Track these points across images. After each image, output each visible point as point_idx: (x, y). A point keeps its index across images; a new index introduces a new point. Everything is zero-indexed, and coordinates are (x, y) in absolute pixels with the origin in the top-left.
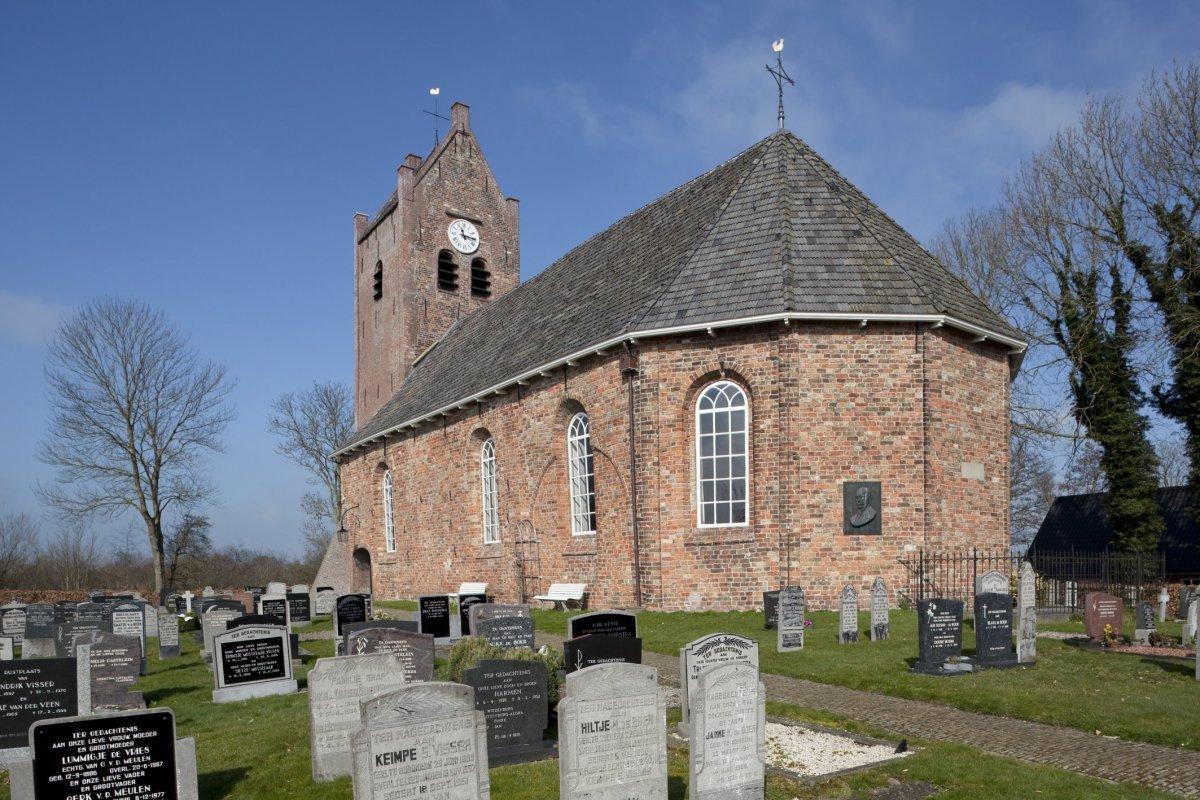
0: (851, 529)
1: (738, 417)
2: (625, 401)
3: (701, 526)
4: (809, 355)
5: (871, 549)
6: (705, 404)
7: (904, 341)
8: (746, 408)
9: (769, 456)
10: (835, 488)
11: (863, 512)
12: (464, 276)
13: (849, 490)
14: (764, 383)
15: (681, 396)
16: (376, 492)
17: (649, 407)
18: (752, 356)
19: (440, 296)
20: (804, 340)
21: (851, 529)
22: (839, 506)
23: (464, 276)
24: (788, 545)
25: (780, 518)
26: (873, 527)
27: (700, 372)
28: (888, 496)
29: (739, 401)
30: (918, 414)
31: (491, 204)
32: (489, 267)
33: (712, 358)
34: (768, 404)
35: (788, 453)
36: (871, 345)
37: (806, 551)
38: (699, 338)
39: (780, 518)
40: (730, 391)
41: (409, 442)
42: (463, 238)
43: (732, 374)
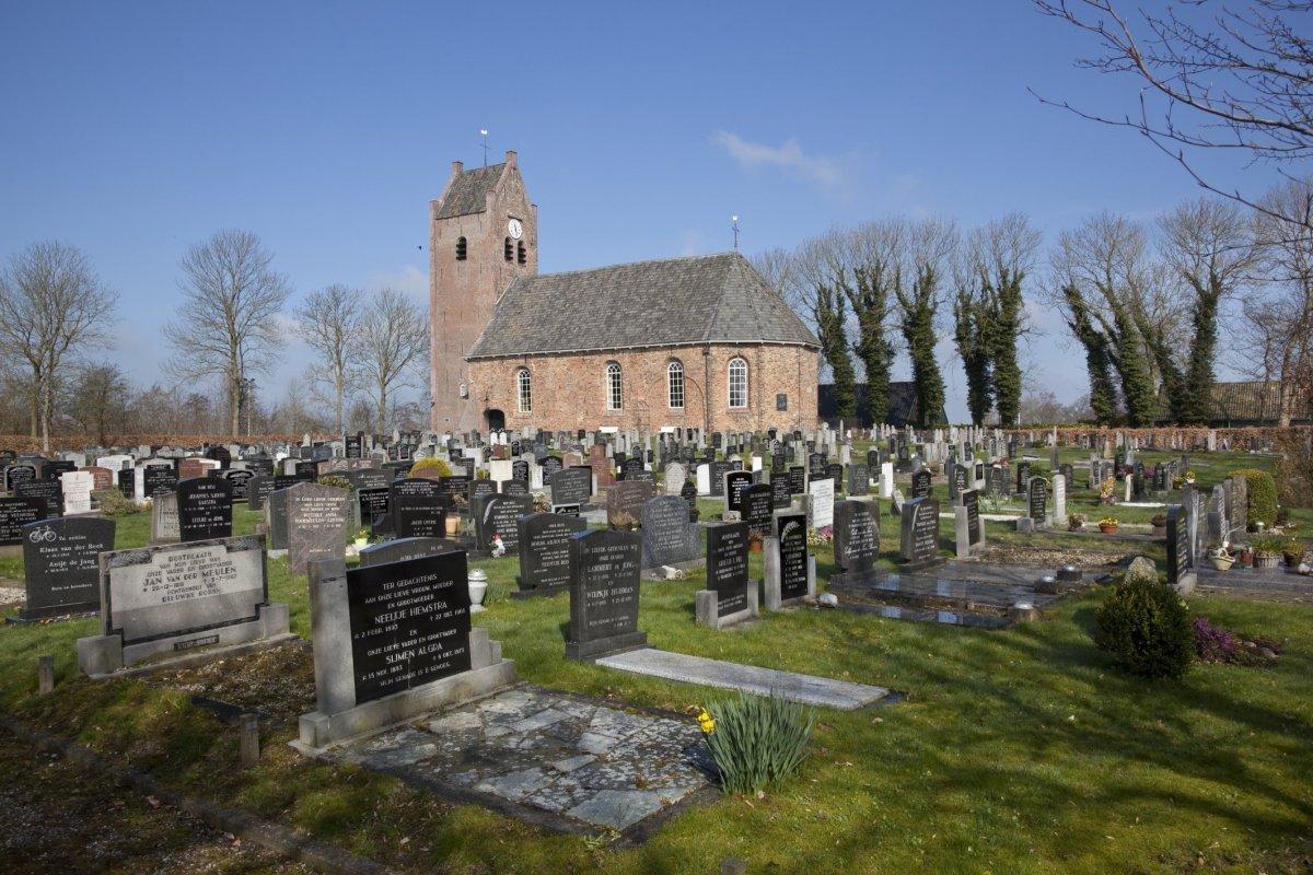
0: (779, 409)
1: (743, 370)
2: (703, 362)
3: (730, 407)
4: (767, 353)
5: (784, 415)
6: (732, 366)
7: (793, 349)
8: (746, 368)
9: (754, 385)
10: (774, 396)
11: (782, 404)
12: (515, 251)
13: (778, 396)
14: (753, 361)
15: (724, 363)
16: (513, 381)
17: (713, 366)
18: (750, 352)
19: (506, 265)
20: (766, 348)
21: (779, 409)
22: (775, 402)
23: (515, 251)
24: (761, 414)
25: (759, 405)
26: (785, 409)
27: (731, 355)
28: (789, 399)
29: (743, 365)
30: (797, 373)
31: (526, 210)
32: (525, 246)
33: (736, 351)
34: (754, 368)
35: (761, 384)
36: (784, 350)
37: (766, 416)
38: (733, 345)
39: (759, 405)
40: (741, 362)
41: (551, 360)
42: (515, 230)
43: (742, 357)
